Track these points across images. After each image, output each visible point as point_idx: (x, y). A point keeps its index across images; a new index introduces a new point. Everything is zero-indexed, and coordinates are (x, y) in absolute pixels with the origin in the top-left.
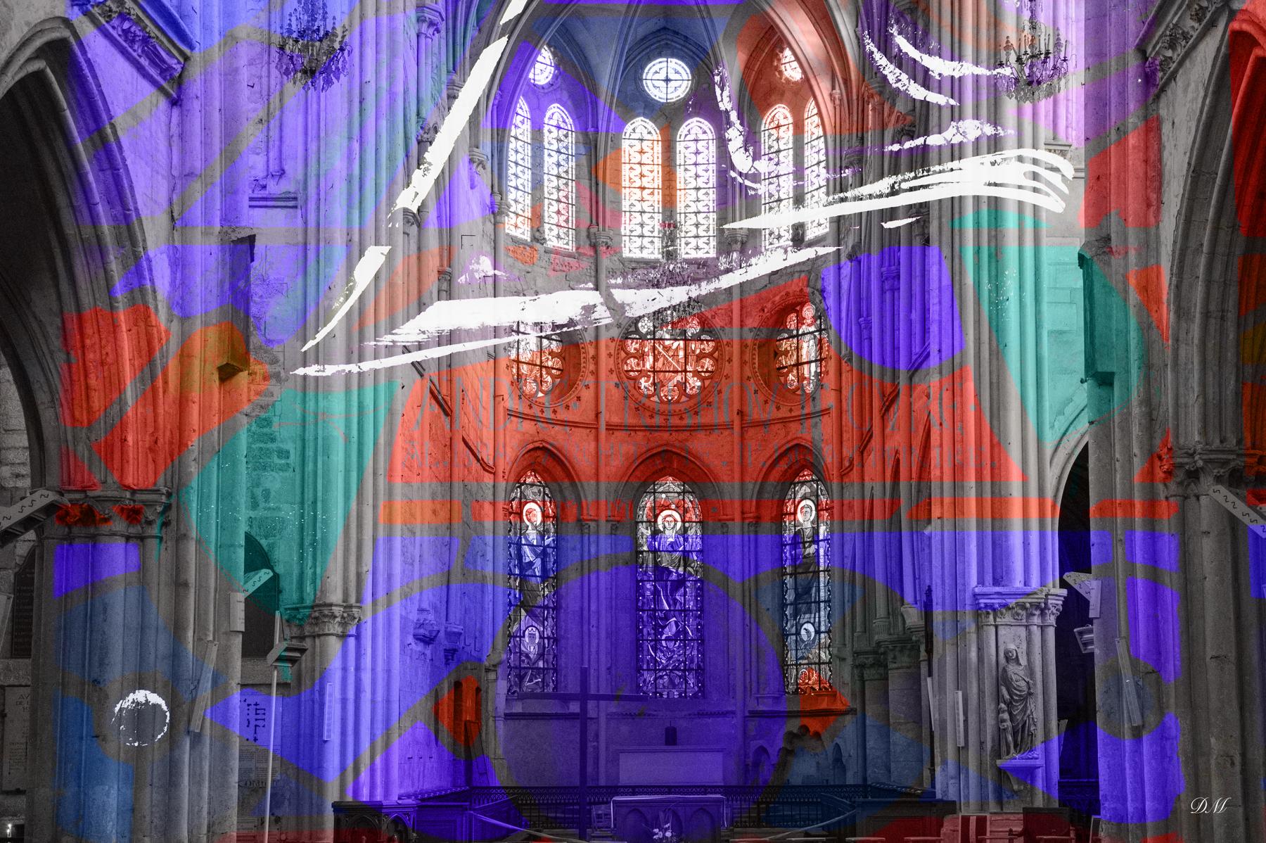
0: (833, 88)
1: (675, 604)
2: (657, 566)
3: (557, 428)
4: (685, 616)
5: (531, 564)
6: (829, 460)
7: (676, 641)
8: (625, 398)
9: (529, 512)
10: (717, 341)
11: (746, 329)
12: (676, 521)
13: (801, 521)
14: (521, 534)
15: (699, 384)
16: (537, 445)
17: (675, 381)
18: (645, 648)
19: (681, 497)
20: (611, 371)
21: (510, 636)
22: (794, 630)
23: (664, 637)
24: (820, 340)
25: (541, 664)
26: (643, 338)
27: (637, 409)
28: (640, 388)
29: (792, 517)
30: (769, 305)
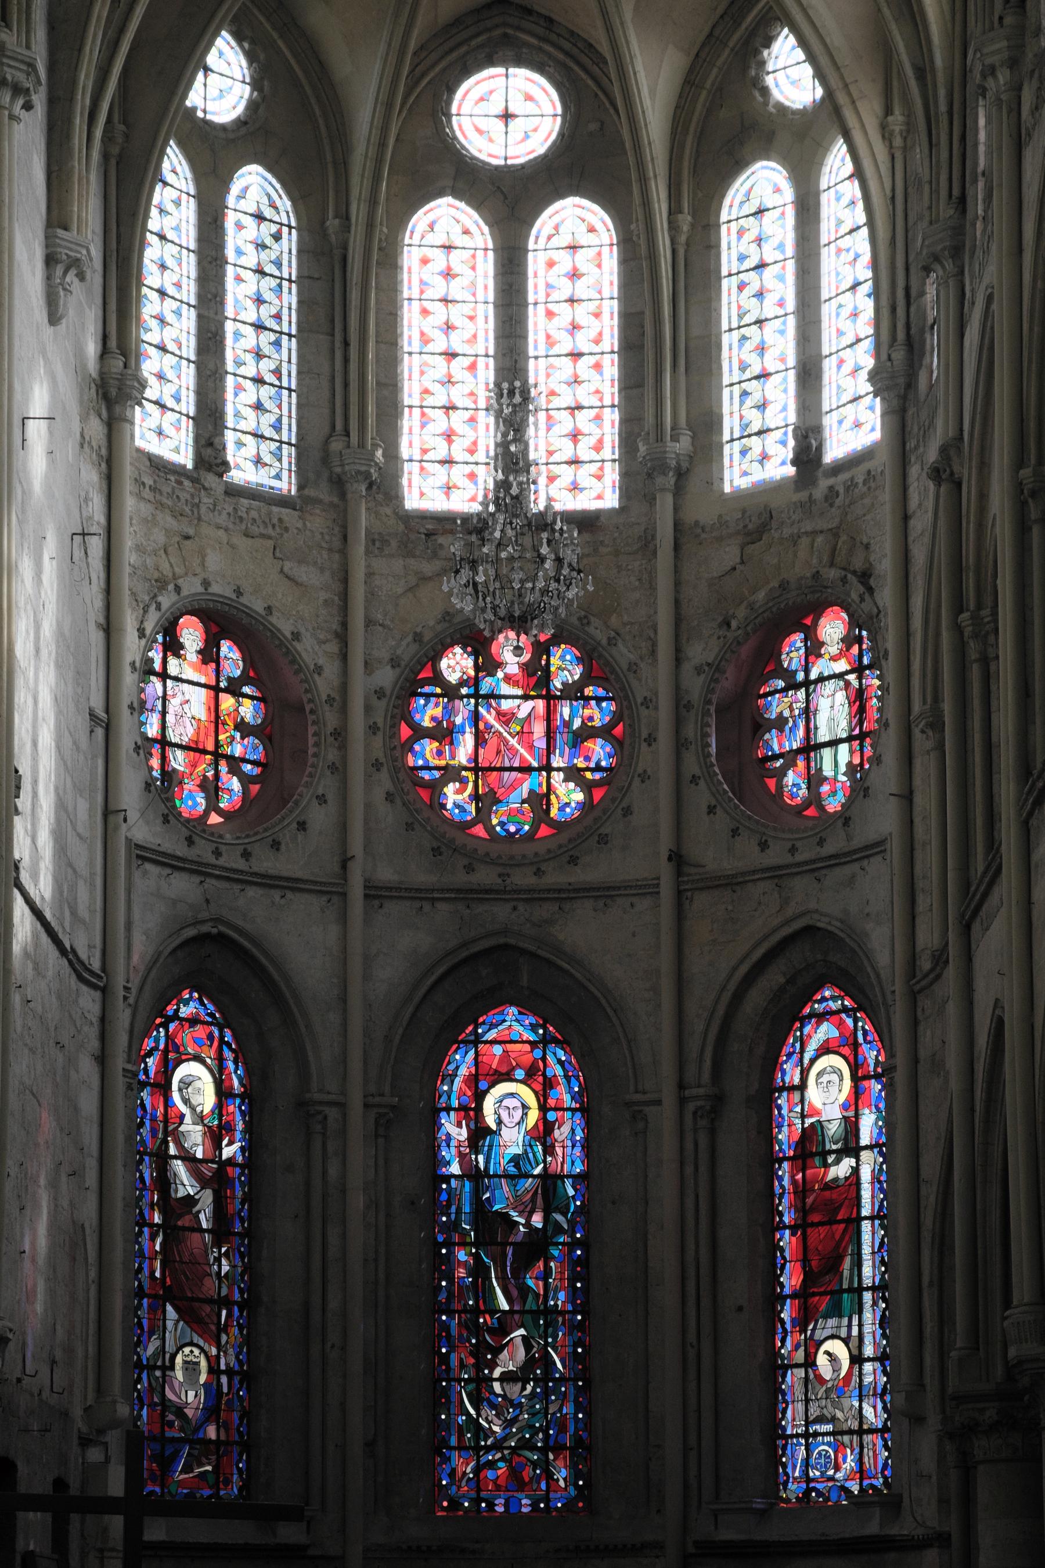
0: (888, 111)
1: (524, 1300)
2: (481, 1210)
3: (252, 892)
4: (547, 1325)
5: (190, 1201)
6: (883, 959)
7: (525, 1382)
8: (409, 827)
9: (185, 1084)
10: (621, 694)
11: (687, 667)
12: (525, 1107)
13: (818, 1104)
14: (166, 1133)
15: (579, 796)
16: (205, 928)
17: (524, 790)
18: (454, 1398)
19: (538, 1053)
20: (377, 765)
21: (139, 1366)
22: (800, 1356)
23: (497, 1373)
24: (860, 693)
25: (211, 1432)
26: (451, 692)
27: (436, 851)
28: (443, 806)
29: (797, 1096)
30: (742, 612)
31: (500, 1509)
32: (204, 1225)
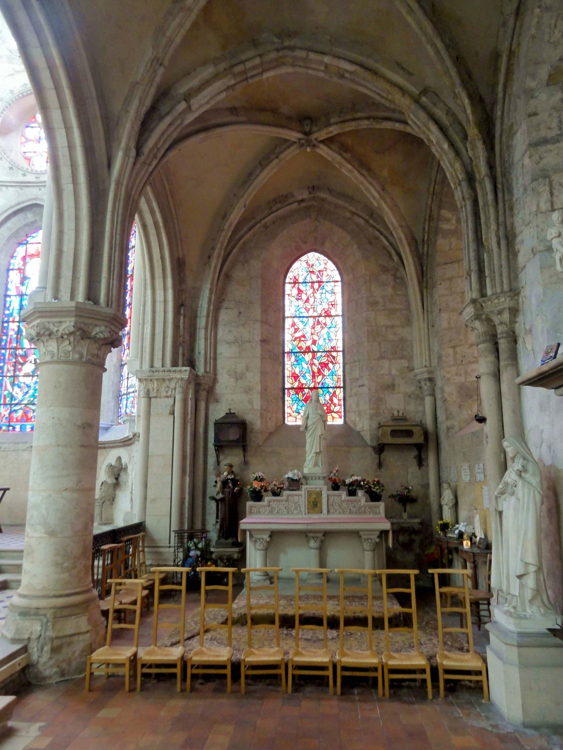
7: (33, 376)
23: (22, 373)
31: (18, 429)
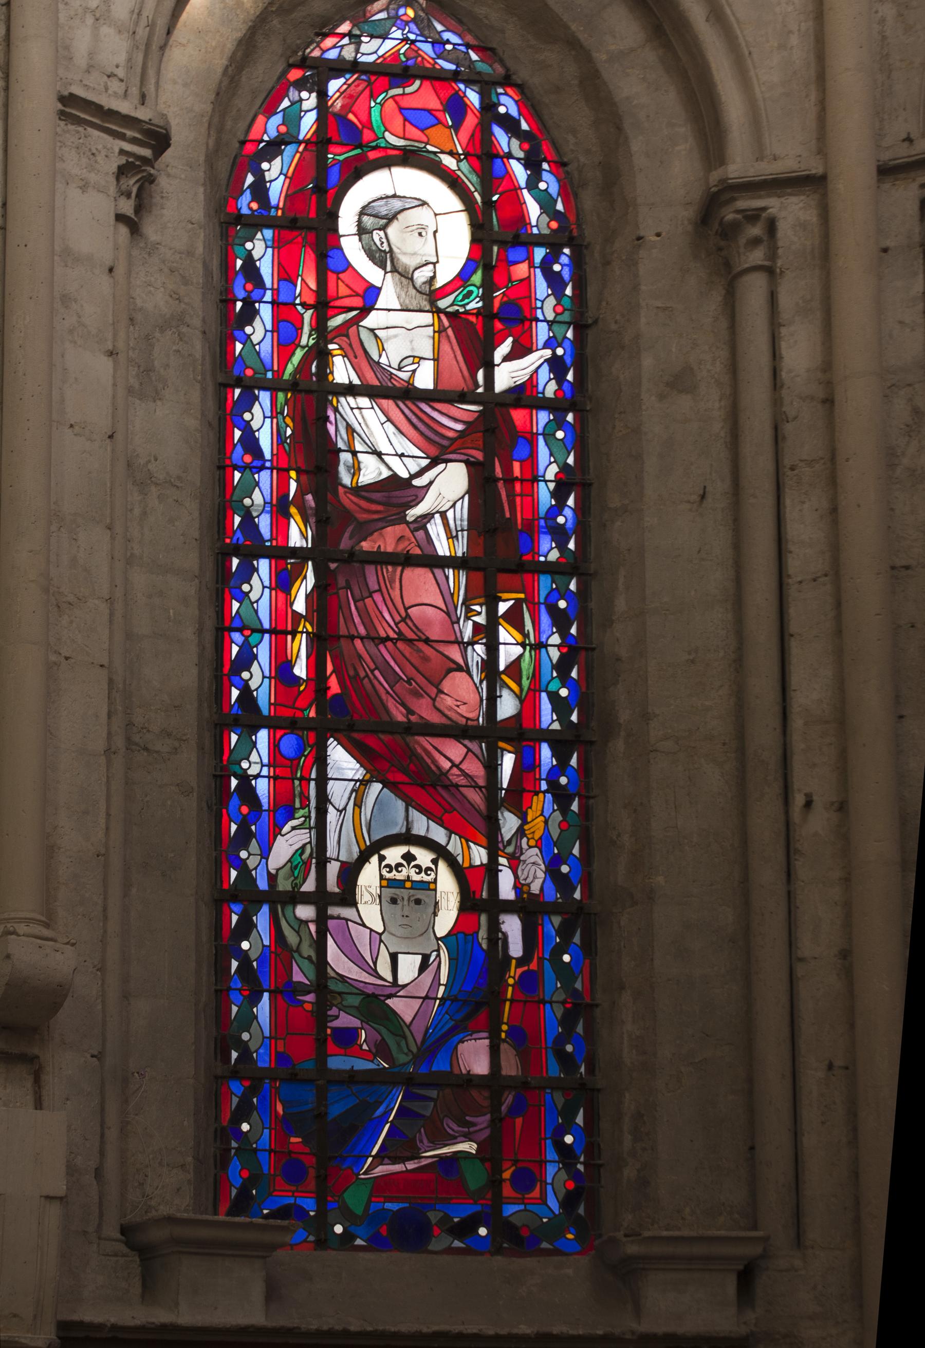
32: (443, 548)
